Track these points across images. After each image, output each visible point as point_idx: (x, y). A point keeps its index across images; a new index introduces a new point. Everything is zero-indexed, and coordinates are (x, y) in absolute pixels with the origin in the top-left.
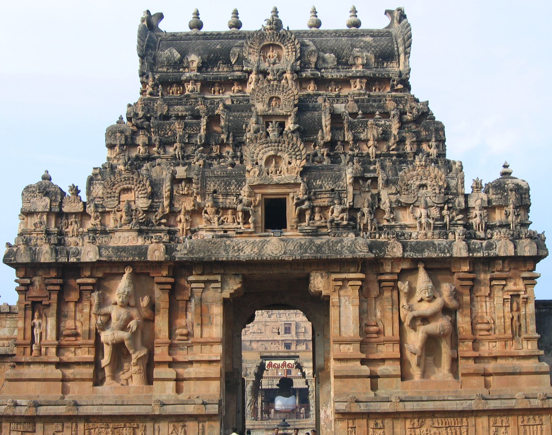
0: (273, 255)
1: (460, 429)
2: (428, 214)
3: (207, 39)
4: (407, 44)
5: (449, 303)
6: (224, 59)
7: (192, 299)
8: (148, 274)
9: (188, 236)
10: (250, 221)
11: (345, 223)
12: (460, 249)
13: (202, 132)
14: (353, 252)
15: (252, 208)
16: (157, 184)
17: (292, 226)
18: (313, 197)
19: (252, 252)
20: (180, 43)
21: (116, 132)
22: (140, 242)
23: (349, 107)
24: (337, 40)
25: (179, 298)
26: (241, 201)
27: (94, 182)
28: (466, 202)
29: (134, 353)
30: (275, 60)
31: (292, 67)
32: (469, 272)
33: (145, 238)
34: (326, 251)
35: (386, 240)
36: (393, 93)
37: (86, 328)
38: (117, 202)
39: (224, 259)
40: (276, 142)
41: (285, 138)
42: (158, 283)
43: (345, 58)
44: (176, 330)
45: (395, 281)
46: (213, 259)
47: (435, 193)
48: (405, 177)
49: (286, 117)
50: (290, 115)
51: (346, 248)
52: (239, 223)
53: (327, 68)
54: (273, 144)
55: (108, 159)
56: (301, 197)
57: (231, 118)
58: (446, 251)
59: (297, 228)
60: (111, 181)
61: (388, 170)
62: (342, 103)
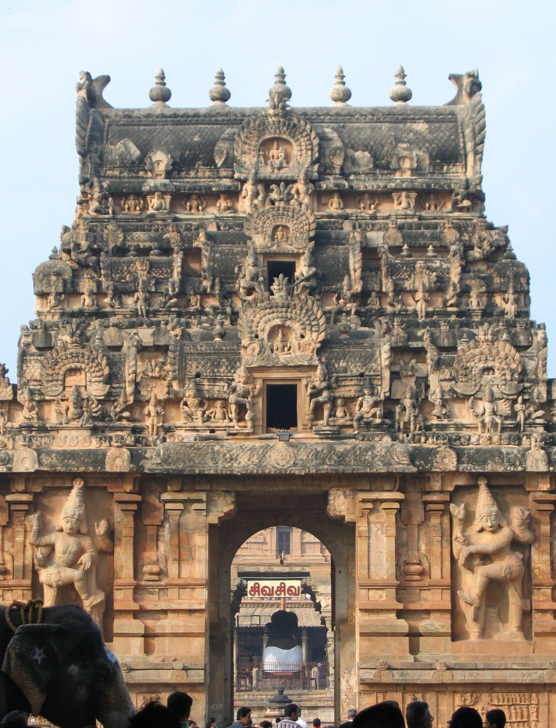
0: (278, 466)
1: (528, 708)
2: (494, 409)
3: (179, 123)
4: (478, 139)
5: (520, 535)
6: (206, 159)
7: (165, 523)
8: (105, 488)
9: (161, 437)
10: (247, 417)
11: (378, 421)
12: (537, 461)
13: (176, 277)
14: (388, 464)
15: (249, 399)
16: (116, 362)
17: (304, 425)
18: (334, 385)
19: (250, 463)
20: (139, 130)
21: (49, 275)
22: (94, 444)
23: (389, 238)
24: (373, 129)
25: (147, 522)
26: (234, 390)
27: (28, 358)
28: (549, 392)
29: (87, 598)
30: (281, 163)
31: (306, 174)
32: (550, 492)
33: (101, 439)
34: (350, 462)
35: (435, 446)
36: (456, 214)
37: (19, 563)
38: (61, 388)
39: (212, 472)
40: (283, 307)
41: (297, 301)
42: (120, 502)
43: (385, 158)
44: (143, 566)
45: (446, 503)
46: (197, 472)
47: (505, 380)
48: (463, 357)
49: (298, 255)
50: (304, 253)
51: (378, 457)
52: (231, 420)
53: (359, 174)
54: (280, 310)
55: (39, 313)
56: (317, 384)
57: (217, 255)
58: (518, 463)
59: (311, 428)
60: (53, 358)
61: (442, 337)
62: (380, 229)
